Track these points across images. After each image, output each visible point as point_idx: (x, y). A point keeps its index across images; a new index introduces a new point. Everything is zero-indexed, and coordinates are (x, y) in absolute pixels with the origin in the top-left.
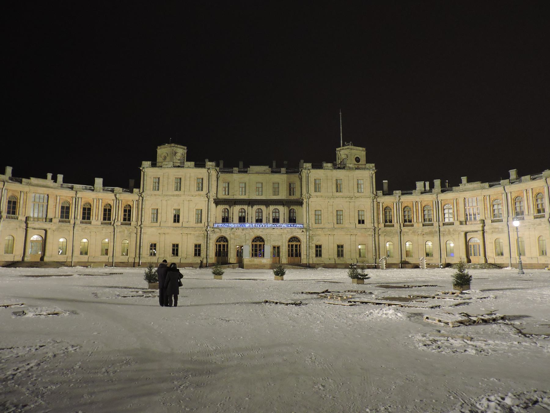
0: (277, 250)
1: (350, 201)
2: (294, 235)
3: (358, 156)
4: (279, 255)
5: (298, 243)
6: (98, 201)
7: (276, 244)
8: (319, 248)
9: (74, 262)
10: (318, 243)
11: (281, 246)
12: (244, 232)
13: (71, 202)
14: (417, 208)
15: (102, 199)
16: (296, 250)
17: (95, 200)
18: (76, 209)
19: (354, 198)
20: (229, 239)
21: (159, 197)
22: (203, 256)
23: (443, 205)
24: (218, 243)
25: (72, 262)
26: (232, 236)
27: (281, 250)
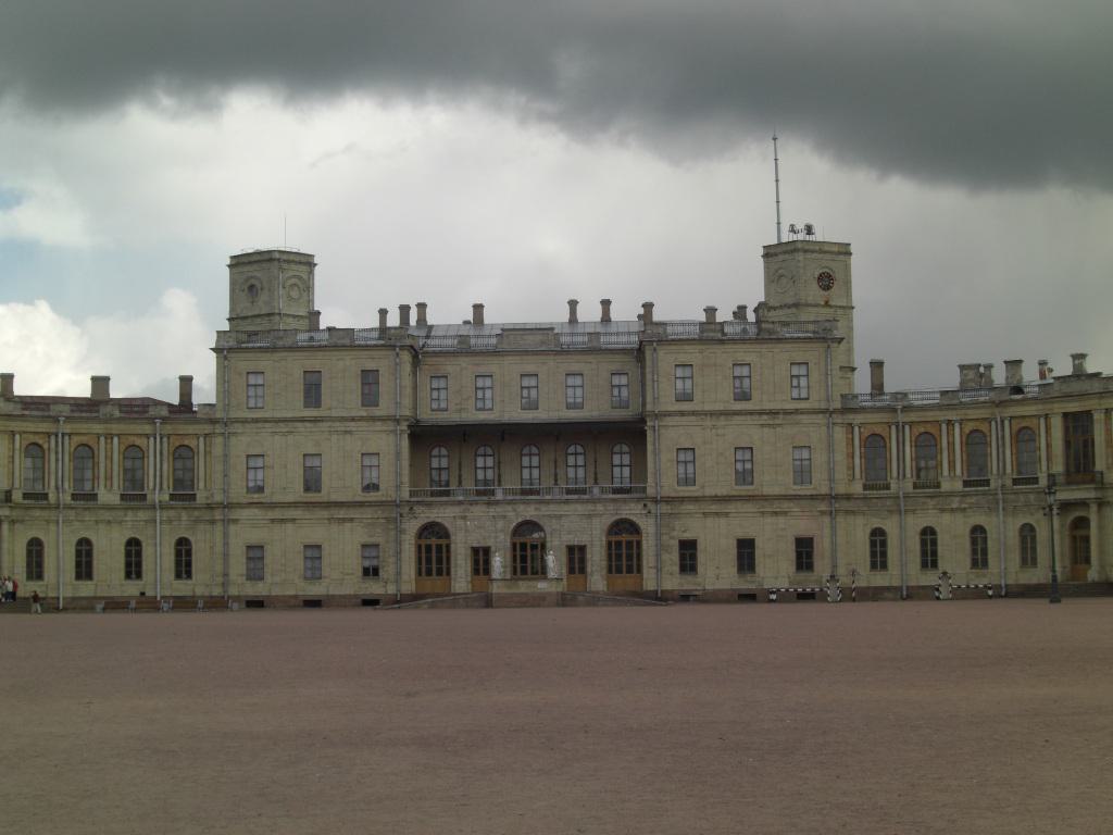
0: (576, 557)
1: (771, 422)
2: (624, 517)
3: (824, 270)
4: (583, 570)
5: (634, 538)
6: (109, 441)
7: (576, 541)
8: (688, 550)
9: (64, 599)
10: (688, 536)
11: (588, 546)
12: (493, 511)
13: (46, 446)
14: (951, 440)
15: (119, 435)
16: (629, 557)
17: (102, 439)
18: (60, 462)
19: (781, 416)
20: (451, 530)
21: (267, 425)
22: (385, 577)
23: (1015, 428)
24: (424, 542)
25: (58, 598)
26: (460, 522)
27: (589, 556)
